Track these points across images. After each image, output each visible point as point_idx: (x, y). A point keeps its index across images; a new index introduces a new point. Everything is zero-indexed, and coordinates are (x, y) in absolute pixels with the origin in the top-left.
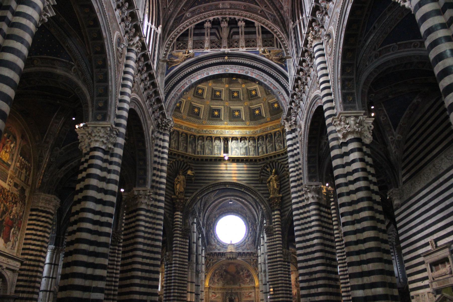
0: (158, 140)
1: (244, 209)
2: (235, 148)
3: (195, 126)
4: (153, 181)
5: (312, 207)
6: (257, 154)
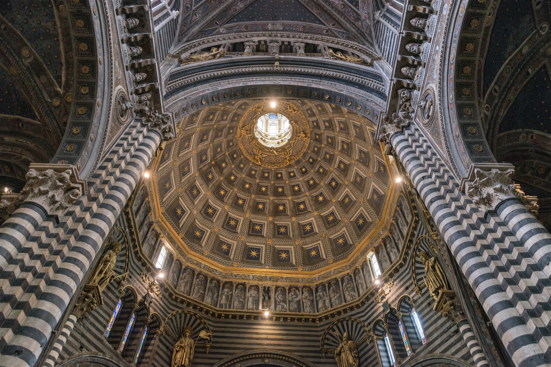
2: (281, 301)
3: (221, 268)
6: (316, 311)
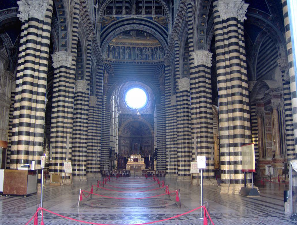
2: (139, 55)
4: (97, 92)
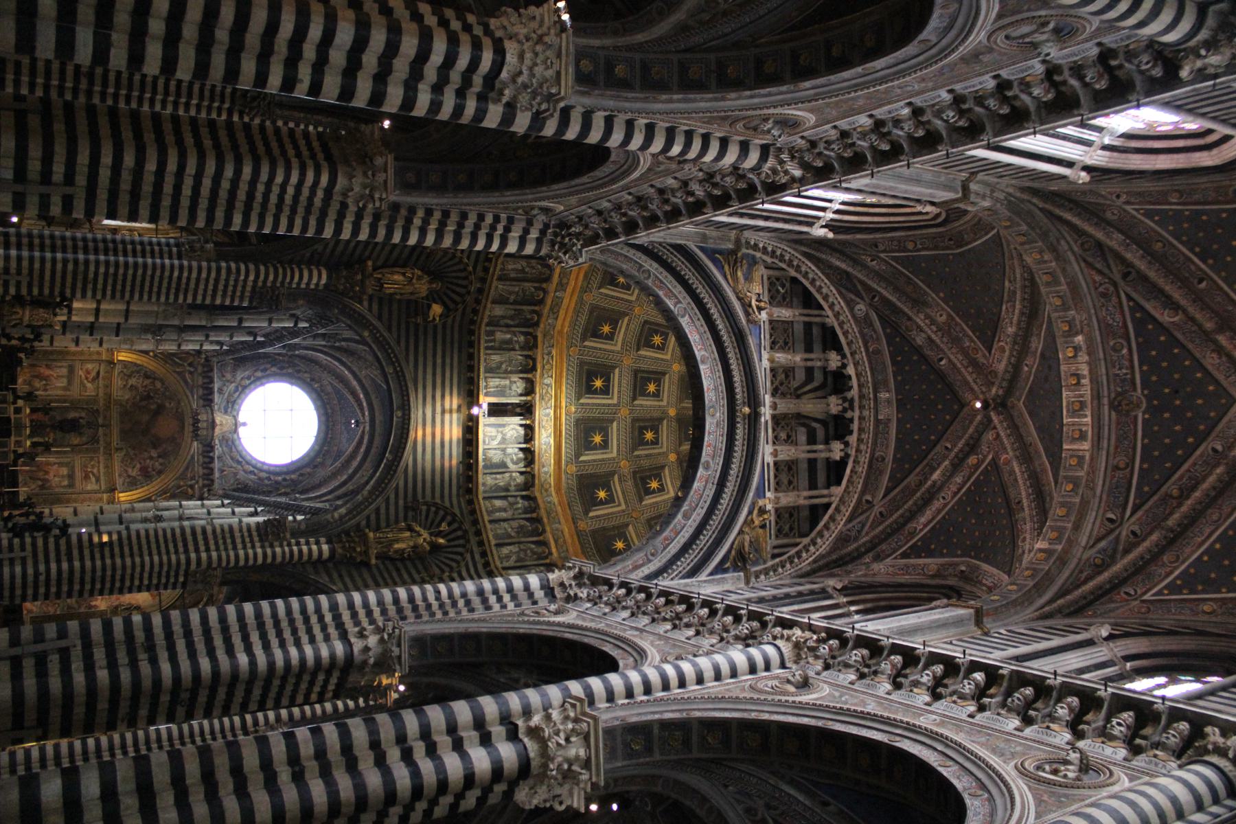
0: (523, 224)
1: (335, 461)
2: (504, 435)
3: (563, 325)
4: (412, 210)
5: (339, 648)
